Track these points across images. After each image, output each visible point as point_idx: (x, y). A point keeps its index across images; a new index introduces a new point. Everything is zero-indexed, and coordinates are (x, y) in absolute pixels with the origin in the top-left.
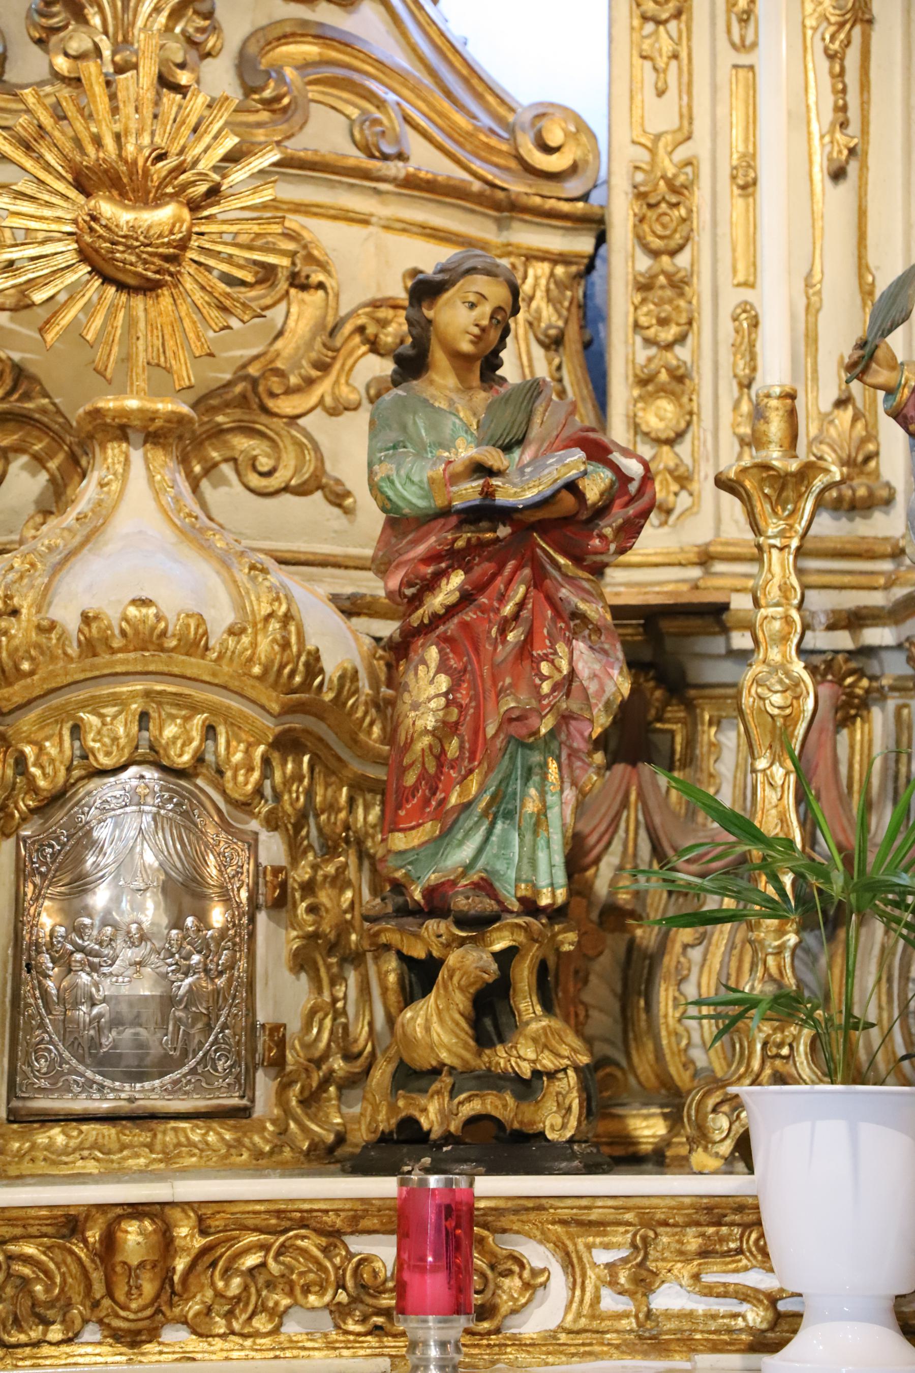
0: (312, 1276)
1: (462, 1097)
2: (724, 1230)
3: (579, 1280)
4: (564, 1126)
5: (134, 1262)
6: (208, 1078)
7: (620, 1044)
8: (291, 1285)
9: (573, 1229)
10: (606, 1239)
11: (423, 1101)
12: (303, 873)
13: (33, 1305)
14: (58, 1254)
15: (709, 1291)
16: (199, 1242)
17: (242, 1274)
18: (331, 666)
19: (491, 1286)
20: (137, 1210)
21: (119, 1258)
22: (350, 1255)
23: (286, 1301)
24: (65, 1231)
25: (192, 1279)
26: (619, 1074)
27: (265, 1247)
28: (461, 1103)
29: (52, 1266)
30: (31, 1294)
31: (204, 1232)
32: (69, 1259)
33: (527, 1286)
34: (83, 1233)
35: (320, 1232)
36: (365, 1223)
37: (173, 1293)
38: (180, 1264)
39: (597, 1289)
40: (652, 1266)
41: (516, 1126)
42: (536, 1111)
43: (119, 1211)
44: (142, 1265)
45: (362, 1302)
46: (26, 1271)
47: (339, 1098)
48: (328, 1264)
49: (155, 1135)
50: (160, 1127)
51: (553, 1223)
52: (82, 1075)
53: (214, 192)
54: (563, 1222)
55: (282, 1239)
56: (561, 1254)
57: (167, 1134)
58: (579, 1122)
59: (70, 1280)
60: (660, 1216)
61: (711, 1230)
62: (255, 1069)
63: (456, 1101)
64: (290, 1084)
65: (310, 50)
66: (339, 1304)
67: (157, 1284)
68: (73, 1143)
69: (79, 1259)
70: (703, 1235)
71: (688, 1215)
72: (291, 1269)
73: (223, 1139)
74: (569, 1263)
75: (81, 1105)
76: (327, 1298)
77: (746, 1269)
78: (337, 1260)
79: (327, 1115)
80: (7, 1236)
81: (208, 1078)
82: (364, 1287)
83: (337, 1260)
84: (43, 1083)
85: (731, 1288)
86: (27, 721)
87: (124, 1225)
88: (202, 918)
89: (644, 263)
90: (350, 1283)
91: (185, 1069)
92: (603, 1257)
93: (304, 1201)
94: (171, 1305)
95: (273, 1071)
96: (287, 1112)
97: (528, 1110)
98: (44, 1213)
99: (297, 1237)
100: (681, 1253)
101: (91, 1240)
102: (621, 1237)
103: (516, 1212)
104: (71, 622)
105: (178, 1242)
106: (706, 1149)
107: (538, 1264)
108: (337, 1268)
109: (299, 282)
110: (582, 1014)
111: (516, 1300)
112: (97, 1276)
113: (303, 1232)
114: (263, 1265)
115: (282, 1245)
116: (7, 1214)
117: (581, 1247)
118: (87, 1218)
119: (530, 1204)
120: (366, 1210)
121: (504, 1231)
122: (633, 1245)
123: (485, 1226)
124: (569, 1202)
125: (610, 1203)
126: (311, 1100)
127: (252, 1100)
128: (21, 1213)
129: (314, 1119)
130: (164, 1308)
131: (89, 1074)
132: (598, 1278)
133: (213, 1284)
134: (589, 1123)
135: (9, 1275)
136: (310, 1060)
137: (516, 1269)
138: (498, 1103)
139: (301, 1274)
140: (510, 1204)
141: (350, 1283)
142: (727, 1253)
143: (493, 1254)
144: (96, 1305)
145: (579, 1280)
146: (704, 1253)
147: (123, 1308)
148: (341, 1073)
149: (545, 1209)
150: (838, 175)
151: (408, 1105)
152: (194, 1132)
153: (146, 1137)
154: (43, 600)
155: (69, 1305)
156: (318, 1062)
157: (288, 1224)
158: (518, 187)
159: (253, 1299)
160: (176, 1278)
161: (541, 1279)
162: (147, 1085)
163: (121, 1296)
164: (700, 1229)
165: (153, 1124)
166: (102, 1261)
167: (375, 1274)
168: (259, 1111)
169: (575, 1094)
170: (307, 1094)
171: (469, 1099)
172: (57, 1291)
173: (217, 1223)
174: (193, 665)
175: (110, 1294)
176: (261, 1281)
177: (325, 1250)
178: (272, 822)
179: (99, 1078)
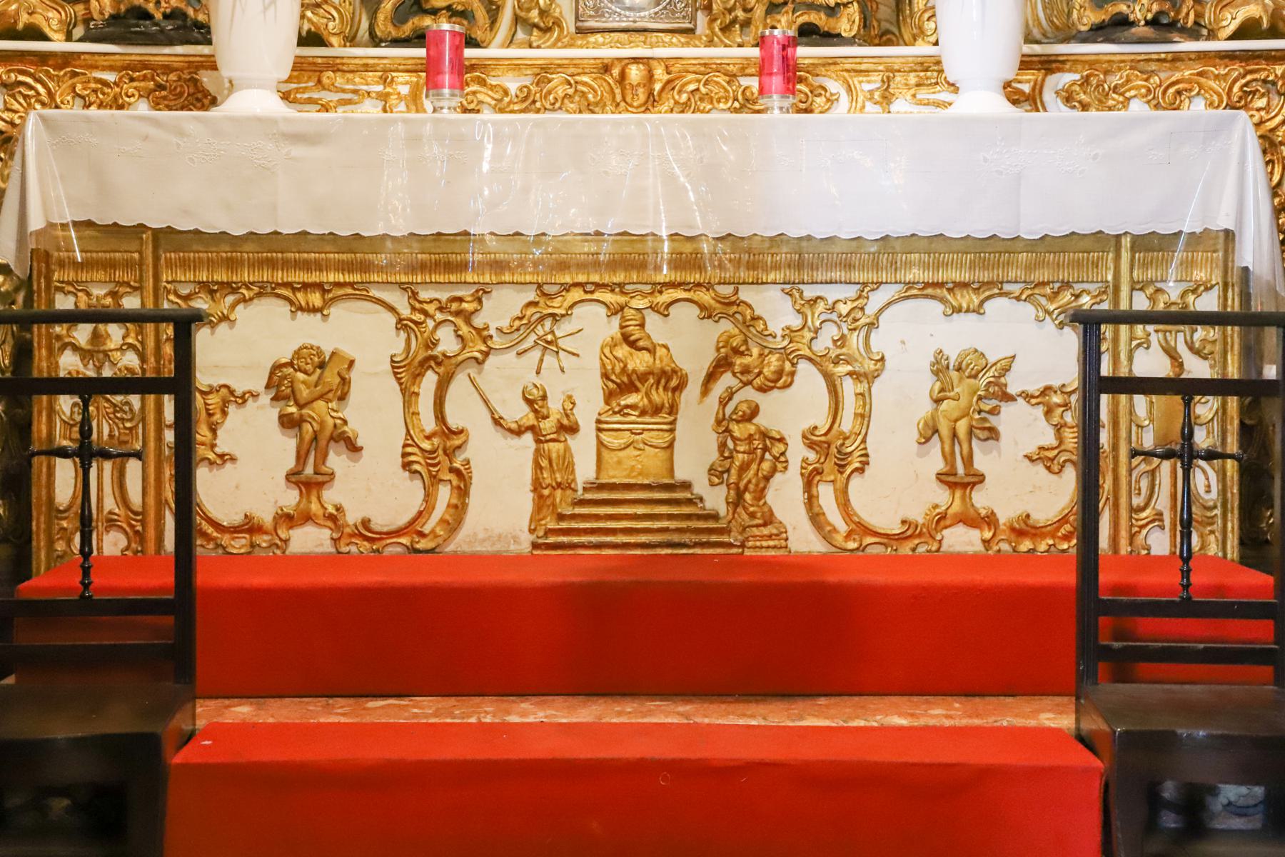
0: (721, 94)
1: (798, 13)
2: (929, 74)
3: (855, 98)
4: (851, 30)
5: (635, 83)
6: (674, 12)
7: (895, 23)
8: (711, 98)
9: (852, 74)
10: (868, 78)
11: (778, 17)
13: (589, 105)
14: (600, 82)
15: (920, 103)
16: (666, 77)
17: (687, 92)
19: (810, 100)
20: (636, 60)
21: (627, 82)
22: (740, 86)
23: (709, 107)
24: (602, 71)
25: (664, 95)
26: (894, 39)
27: (699, 81)
28: (798, 17)
29: (596, 86)
30: (587, 99)
31: (669, 73)
32: (604, 84)
33: (828, 100)
34: (610, 71)
35: (725, 74)
36: (748, 71)
37: (654, 101)
38: (658, 87)
39: (864, 102)
40: (891, 91)
41: (826, 29)
42: (837, 23)
43: (627, 61)
44: (639, 85)
45: (746, 106)
46: (584, 89)
47: (741, 31)
48: (729, 88)
49: (646, 38)
50: (649, 35)
51: (842, 71)
52: (610, 9)
54: (848, 71)
55: (707, 77)
56: (845, 85)
58: (859, 29)
59: (605, 94)
60: (896, 67)
61: (922, 74)
62: (697, 10)
63: (795, 16)
64: (715, 20)
66: (735, 108)
67: (646, 95)
68: (607, 41)
69: (609, 84)
70: (918, 76)
71: (911, 67)
72: (712, 92)
73: (680, 41)
74: (849, 89)
76: (729, 104)
77: (939, 92)
78: (734, 88)
79: (734, 37)
80: (575, 73)
81: (674, 12)
82: (747, 100)
83: (734, 88)
84: (592, 13)
85: (931, 101)
87: (629, 66)
90: (740, 97)
91: (661, 7)
92: (867, 87)
93: (718, 58)
94: (653, 106)
95: (706, 12)
96: (713, 33)
97: (832, 21)
98: (592, 61)
99: (714, 76)
100: (906, 85)
101: (614, 75)
102: (876, 78)
103: (824, 65)
105: (656, 77)
106: (923, 39)
107: (834, 91)
108: (734, 91)
110: (874, 7)
111: (823, 107)
112: (618, 91)
113: (717, 74)
114: (698, 89)
115: (707, 80)
116: (575, 62)
117: (856, 82)
118: (612, 65)
119: (830, 61)
120: (748, 64)
121: (817, 75)
122: (883, 81)
123: (808, 72)
124: (850, 60)
125: (871, 60)
127: (695, 26)
128: (581, 61)
129: (727, 38)
130: (650, 108)
131: (613, 7)
132: (865, 97)
133: (673, 98)
134: (865, 31)
135: (576, 91)
136: (725, 9)
137: (823, 92)
138: (816, 17)
139: (716, 93)
140: (820, 61)
141: (740, 97)
142: (930, 84)
143: (812, 85)
144: (618, 105)
145: (855, 98)
146: (918, 85)
147: (631, 106)
148: (741, 18)
149: (838, 64)
151: (772, 21)
153: (642, 38)
155: (605, 105)
156: (730, 11)
157: (710, 70)
159: (693, 105)
160: (655, 93)
161: (836, 97)
162: (642, 14)
163: (629, 99)
164: (918, 73)
165: (646, 33)
166: (620, 84)
167: (753, 94)
168: (698, 32)
169: (857, 14)
170: (723, 25)
171: (802, 15)
172: (599, 98)
173: (673, 69)
175: (624, 99)
176: (697, 97)
177: (728, 83)
179: (618, 10)
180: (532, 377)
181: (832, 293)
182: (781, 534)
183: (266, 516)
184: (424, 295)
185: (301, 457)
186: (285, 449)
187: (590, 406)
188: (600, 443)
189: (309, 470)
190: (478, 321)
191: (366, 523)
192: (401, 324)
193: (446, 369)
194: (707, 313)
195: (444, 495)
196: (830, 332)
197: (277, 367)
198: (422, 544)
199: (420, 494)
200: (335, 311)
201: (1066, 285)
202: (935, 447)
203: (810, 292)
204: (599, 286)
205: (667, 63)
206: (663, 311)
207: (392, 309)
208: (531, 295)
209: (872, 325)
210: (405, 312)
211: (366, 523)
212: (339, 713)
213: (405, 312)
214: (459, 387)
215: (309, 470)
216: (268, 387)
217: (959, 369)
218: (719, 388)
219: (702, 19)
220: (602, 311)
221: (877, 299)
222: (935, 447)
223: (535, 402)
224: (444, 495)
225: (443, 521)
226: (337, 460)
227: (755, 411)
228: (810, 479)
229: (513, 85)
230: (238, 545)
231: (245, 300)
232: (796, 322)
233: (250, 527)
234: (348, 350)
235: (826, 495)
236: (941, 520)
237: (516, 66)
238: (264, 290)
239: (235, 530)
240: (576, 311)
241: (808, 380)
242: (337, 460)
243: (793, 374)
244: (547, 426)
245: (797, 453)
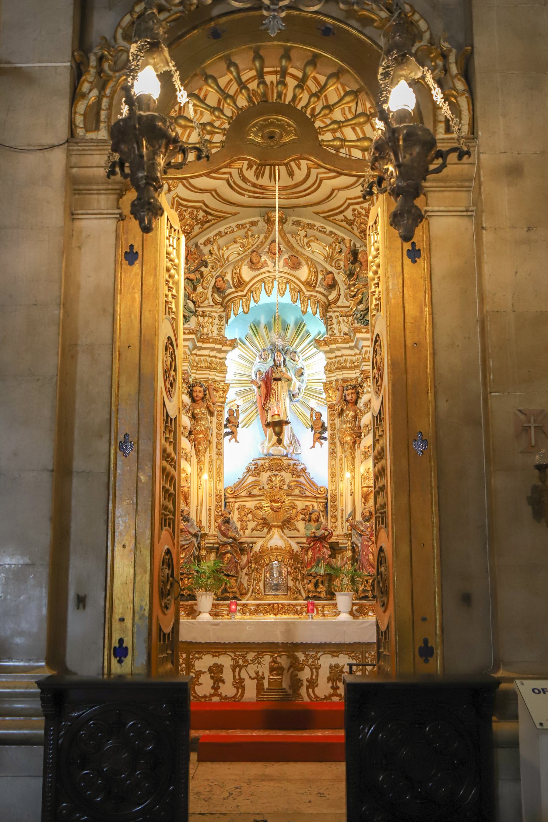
12: (292, 571)
18: (295, 551)
53: (284, 502)
57: (279, 597)
65: (295, 483)
75: (271, 594)
86: (265, 557)
88: (282, 576)
89: (332, 503)
104: (269, 547)
109: (294, 508)
126: (294, 594)
150: (351, 495)
152: (282, 596)
154: (267, 545)
158: (318, 496)
174: (281, 551)
178: (289, 566)
180: (256, 668)
181: (311, 653)
182: (302, 698)
183: (208, 695)
184: (237, 653)
185: (214, 684)
186: (211, 682)
187: (267, 674)
188: (269, 681)
189: (216, 686)
190: (247, 658)
191: (226, 696)
192: (233, 659)
193: (241, 667)
194: (288, 657)
195: (240, 690)
196: (311, 660)
197: (210, 667)
198: (236, 700)
199: (236, 690)
200: (220, 657)
201: (353, 652)
202: (331, 682)
203: (307, 653)
204: (269, 652)
205: (282, 604)
206: (280, 656)
207: (231, 656)
208: (256, 654)
209: (319, 659)
210: (233, 657)
211: (226, 696)
212: (223, 733)
213: (233, 657)
214: (243, 670)
215: (216, 686)
216: (208, 671)
217: (334, 667)
218: (290, 671)
219: (289, 592)
220: (269, 656)
221: (319, 654)
222: (331, 682)
223: (257, 673)
224: (240, 690)
225: (240, 696)
226: (221, 684)
227: (297, 675)
228: (308, 687)
229: (252, 608)
230: (203, 700)
231: (205, 655)
232: (305, 659)
233: (205, 696)
234: (223, 664)
235: (310, 690)
236: (331, 695)
237: (253, 605)
238: (208, 653)
239: (202, 697)
240: (265, 657)
241: (307, 670)
242: (221, 684)
243: (304, 668)
244: (259, 677)
245: (305, 683)
